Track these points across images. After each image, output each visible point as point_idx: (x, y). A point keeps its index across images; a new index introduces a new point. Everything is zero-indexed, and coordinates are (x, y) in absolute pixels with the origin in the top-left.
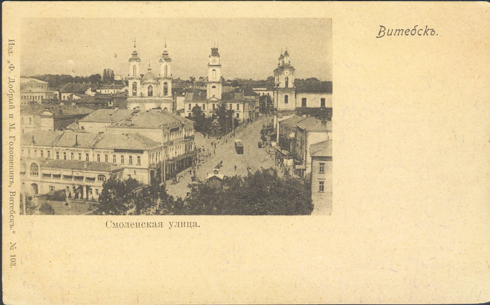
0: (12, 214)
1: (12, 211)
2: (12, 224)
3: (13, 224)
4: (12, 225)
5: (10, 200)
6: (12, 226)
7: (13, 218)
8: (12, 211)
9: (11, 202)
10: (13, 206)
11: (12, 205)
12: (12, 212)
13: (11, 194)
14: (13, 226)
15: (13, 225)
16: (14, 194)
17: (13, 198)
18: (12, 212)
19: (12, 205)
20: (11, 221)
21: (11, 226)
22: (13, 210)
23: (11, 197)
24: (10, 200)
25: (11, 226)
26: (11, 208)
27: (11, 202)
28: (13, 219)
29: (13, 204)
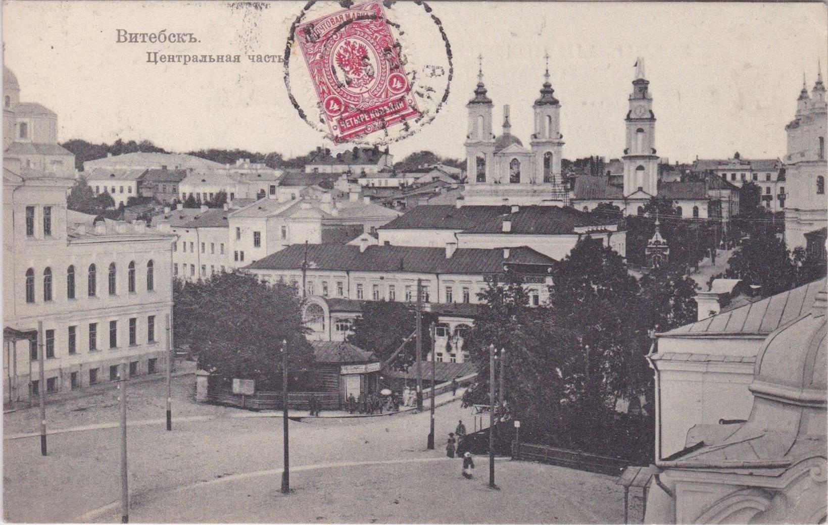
0: (167, 39)
1: (159, 36)
2: (187, 38)
4: (191, 38)
5: (136, 41)
6: (193, 40)
7: (174, 36)
8: (159, 36)
9: (140, 39)
10: (149, 35)
11: (147, 39)
13: (122, 39)
14: (193, 36)
15: (191, 35)
16: (122, 33)
17: (131, 35)
19: (147, 39)
20: (181, 40)
21: (193, 40)
22: (157, 36)
23: (129, 39)
25: (193, 40)
26: (153, 40)
28: (177, 36)
29: (144, 35)
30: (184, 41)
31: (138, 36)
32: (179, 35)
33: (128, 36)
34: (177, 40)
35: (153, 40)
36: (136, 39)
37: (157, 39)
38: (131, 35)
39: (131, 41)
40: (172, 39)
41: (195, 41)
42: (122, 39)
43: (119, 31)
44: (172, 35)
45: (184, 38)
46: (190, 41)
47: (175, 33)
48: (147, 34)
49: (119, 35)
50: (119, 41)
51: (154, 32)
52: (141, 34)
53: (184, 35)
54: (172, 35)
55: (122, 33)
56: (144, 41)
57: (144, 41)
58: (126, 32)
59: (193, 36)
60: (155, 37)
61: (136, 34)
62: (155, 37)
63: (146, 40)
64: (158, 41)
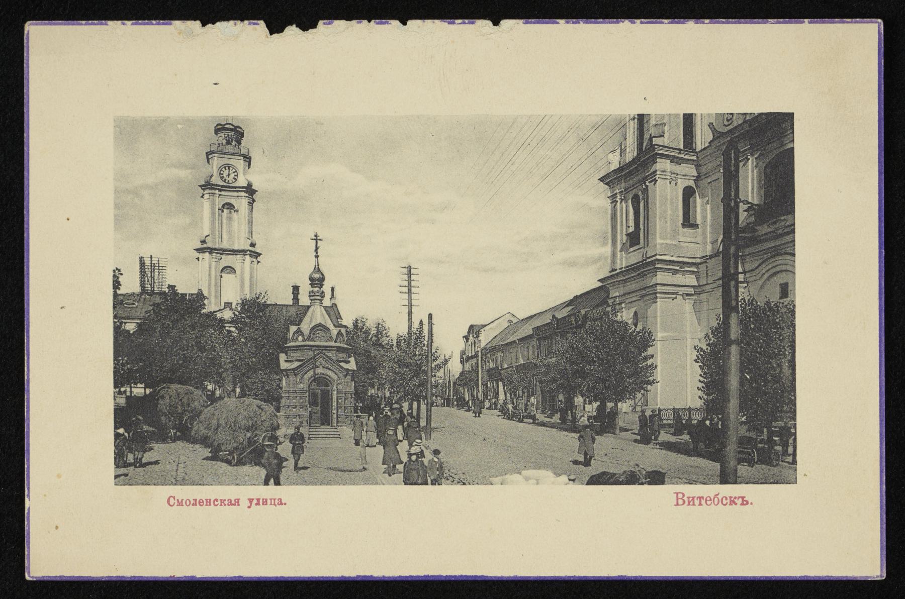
2: (739, 501)
3: (740, 499)
4: (743, 500)
5: (694, 504)
7: (726, 499)
9: (697, 502)
10: (704, 499)
11: (703, 502)
12: (716, 499)
13: (680, 502)
14: (745, 499)
15: (743, 498)
16: (680, 496)
17: (689, 498)
18: (716, 500)
22: (712, 498)
23: (687, 503)
24: (694, 504)
26: (709, 503)
27: (697, 502)
28: (729, 498)
30: (736, 504)
31: (695, 499)
32: (731, 497)
33: (686, 498)
34: (729, 503)
35: (709, 503)
36: (694, 502)
37: (712, 501)
38: (689, 498)
39: (689, 504)
40: (724, 502)
41: (747, 503)
42: (680, 502)
43: (677, 494)
44: (724, 499)
45: (736, 500)
46: (742, 504)
47: (727, 496)
48: (703, 497)
49: (678, 499)
50: (677, 504)
51: (710, 496)
52: (739, 497)
53: (735, 498)
54: (724, 499)
55: (680, 496)
56: (700, 504)
57: (700, 504)
58: (684, 495)
59: (745, 499)
60: (710, 500)
61: (693, 498)
62: (710, 500)
63: (702, 503)
64: (713, 504)
